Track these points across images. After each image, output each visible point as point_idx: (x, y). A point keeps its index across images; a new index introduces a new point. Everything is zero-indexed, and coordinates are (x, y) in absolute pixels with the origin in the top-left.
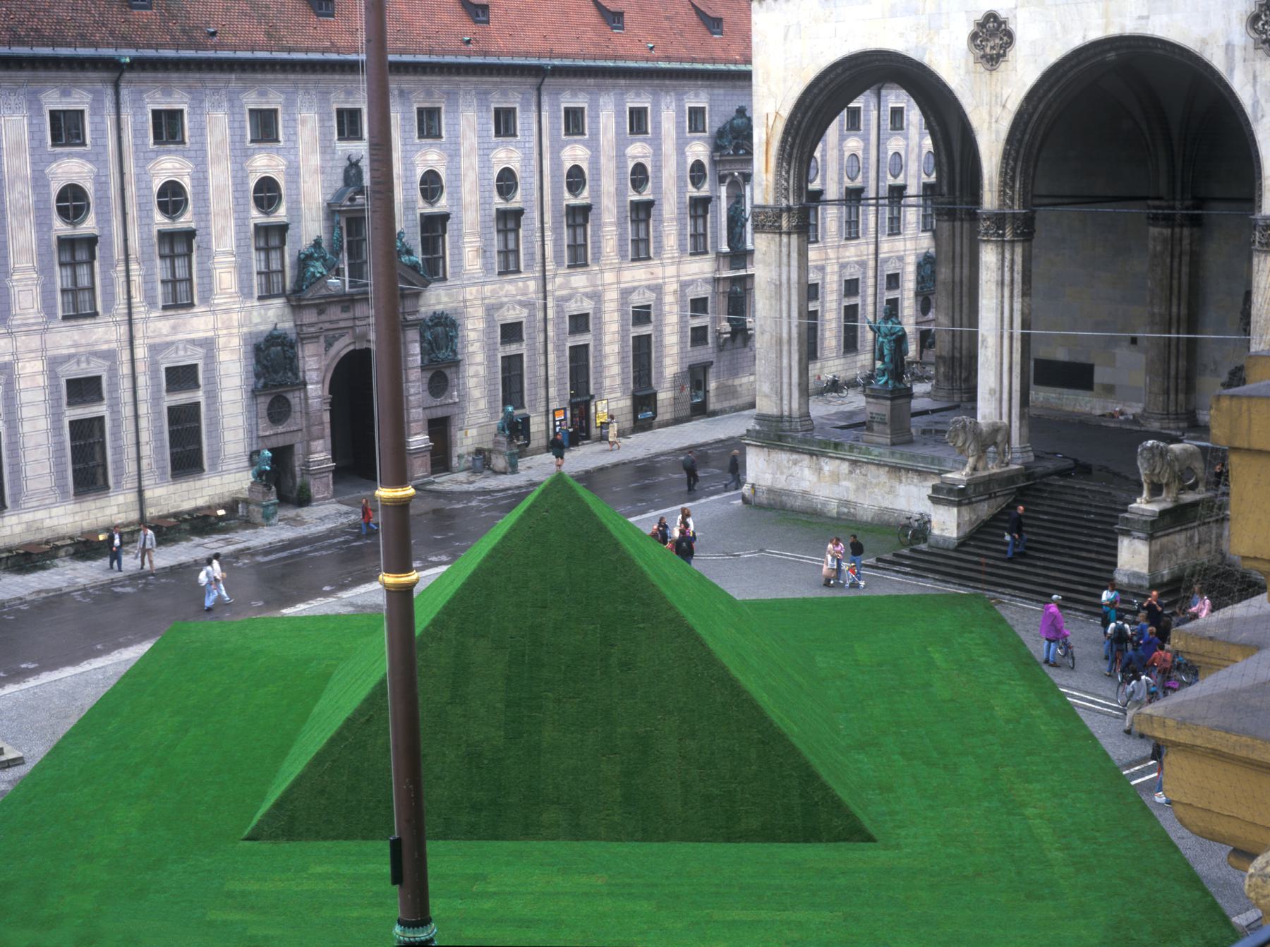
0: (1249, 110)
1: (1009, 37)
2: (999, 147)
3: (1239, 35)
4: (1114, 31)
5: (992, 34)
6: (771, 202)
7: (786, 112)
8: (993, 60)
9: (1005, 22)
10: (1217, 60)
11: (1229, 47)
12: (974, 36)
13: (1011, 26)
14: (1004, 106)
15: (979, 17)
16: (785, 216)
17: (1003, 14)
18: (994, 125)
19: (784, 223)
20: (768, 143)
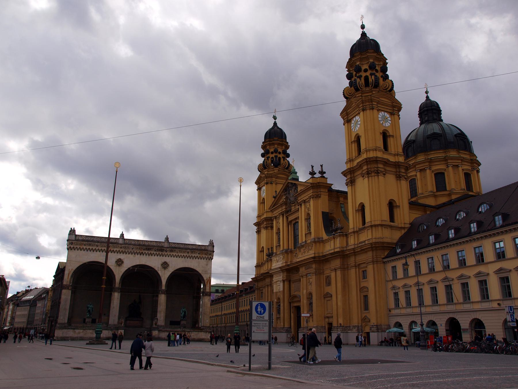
0: (161, 276)
1: (123, 262)
2: (120, 278)
3: (160, 266)
4: (141, 263)
5: (120, 261)
6: (68, 284)
7: (74, 269)
8: (119, 265)
9: (122, 260)
10: (156, 269)
11: (158, 268)
12: (116, 261)
13: (123, 261)
14: (121, 272)
15: (118, 259)
16: (70, 287)
17: (122, 259)
18: (119, 275)
19: (70, 288)
20: (69, 274)
